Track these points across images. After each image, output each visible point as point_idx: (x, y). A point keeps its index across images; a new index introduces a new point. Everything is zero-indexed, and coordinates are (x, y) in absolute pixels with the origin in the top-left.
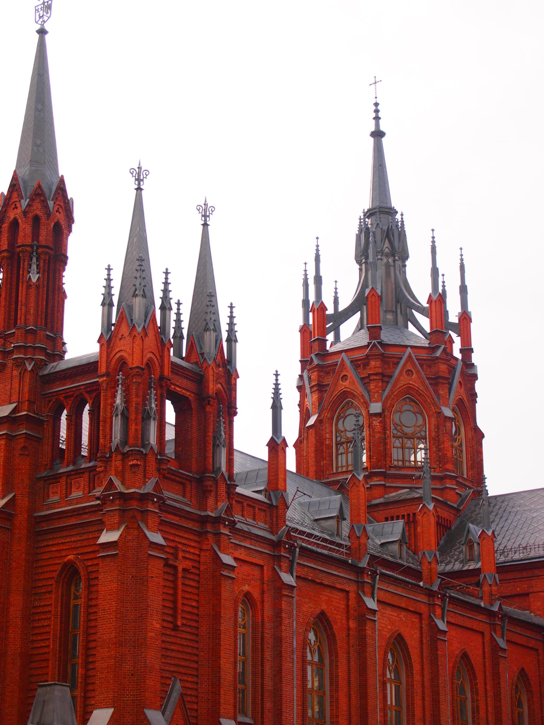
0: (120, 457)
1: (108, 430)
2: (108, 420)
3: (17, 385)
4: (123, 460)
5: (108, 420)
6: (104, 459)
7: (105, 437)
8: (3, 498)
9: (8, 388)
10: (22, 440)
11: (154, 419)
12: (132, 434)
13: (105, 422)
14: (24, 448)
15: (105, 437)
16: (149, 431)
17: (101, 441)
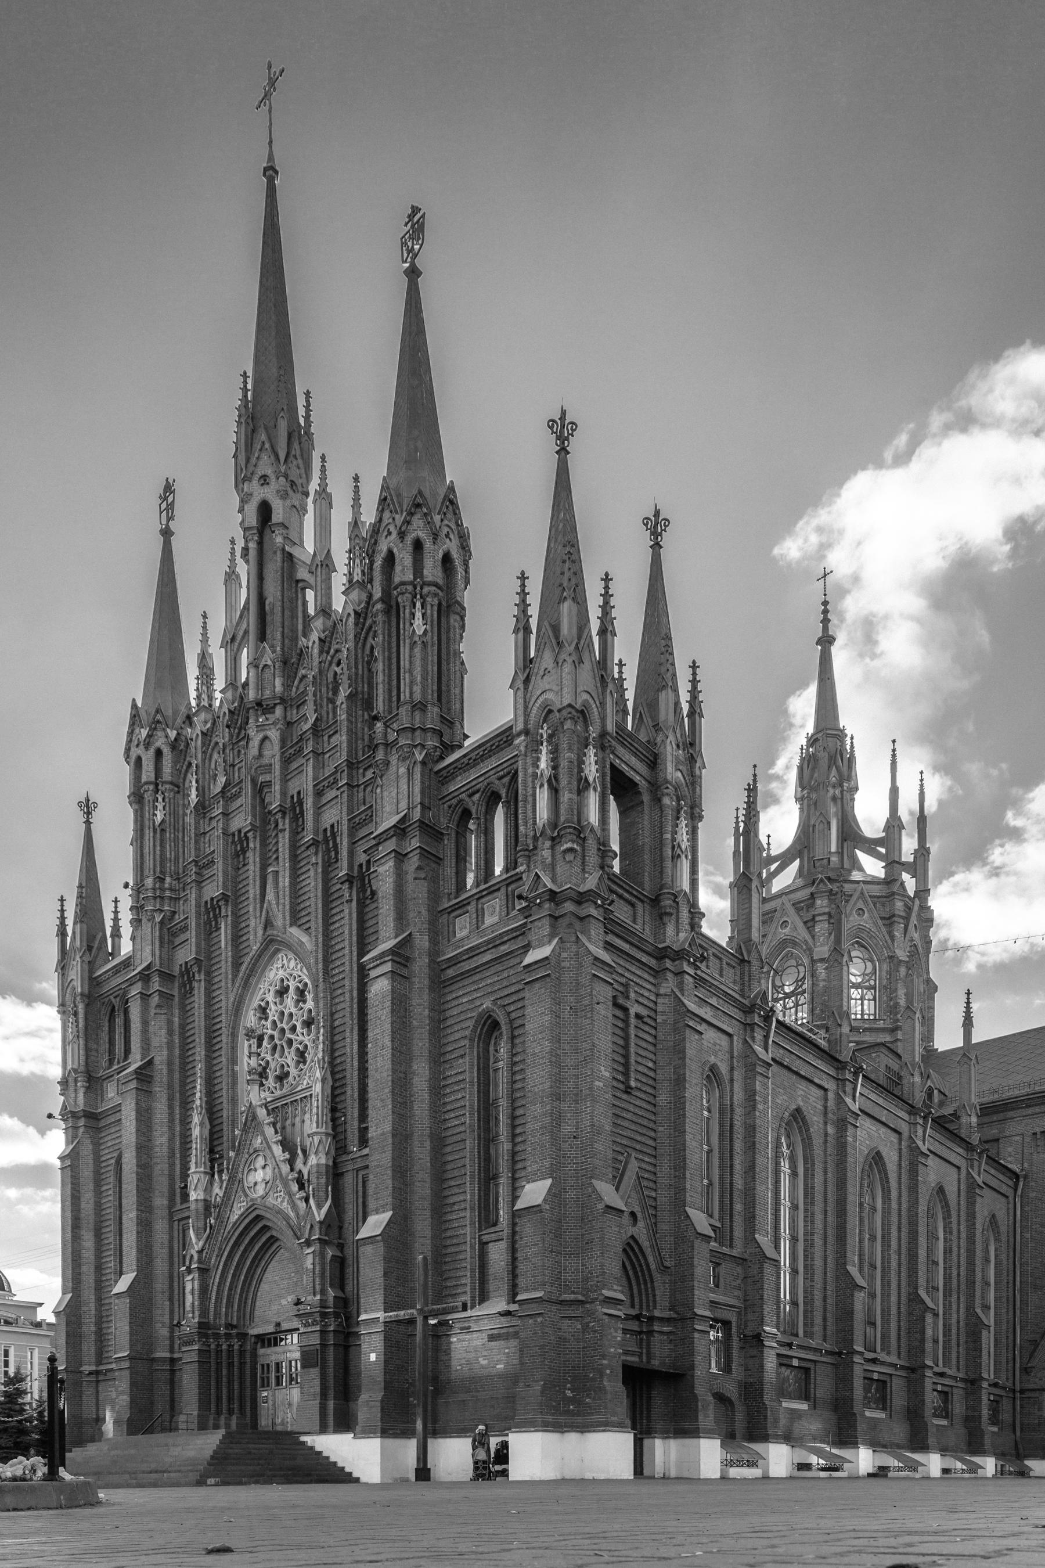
0: (548, 844)
1: (530, 813)
2: (530, 799)
3: (405, 787)
4: (553, 848)
5: (530, 799)
6: (527, 853)
7: (526, 823)
8: (396, 937)
9: (394, 794)
10: (416, 858)
11: (595, 789)
12: (563, 808)
13: (525, 801)
14: (419, 868)
15: (526, 823)
16: (588, 805)
17: (521, 828)
